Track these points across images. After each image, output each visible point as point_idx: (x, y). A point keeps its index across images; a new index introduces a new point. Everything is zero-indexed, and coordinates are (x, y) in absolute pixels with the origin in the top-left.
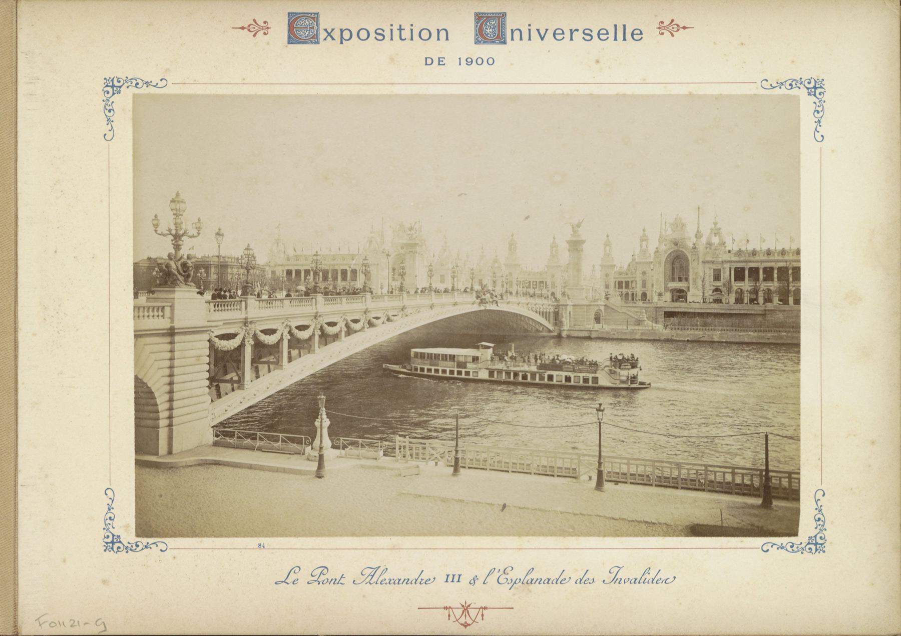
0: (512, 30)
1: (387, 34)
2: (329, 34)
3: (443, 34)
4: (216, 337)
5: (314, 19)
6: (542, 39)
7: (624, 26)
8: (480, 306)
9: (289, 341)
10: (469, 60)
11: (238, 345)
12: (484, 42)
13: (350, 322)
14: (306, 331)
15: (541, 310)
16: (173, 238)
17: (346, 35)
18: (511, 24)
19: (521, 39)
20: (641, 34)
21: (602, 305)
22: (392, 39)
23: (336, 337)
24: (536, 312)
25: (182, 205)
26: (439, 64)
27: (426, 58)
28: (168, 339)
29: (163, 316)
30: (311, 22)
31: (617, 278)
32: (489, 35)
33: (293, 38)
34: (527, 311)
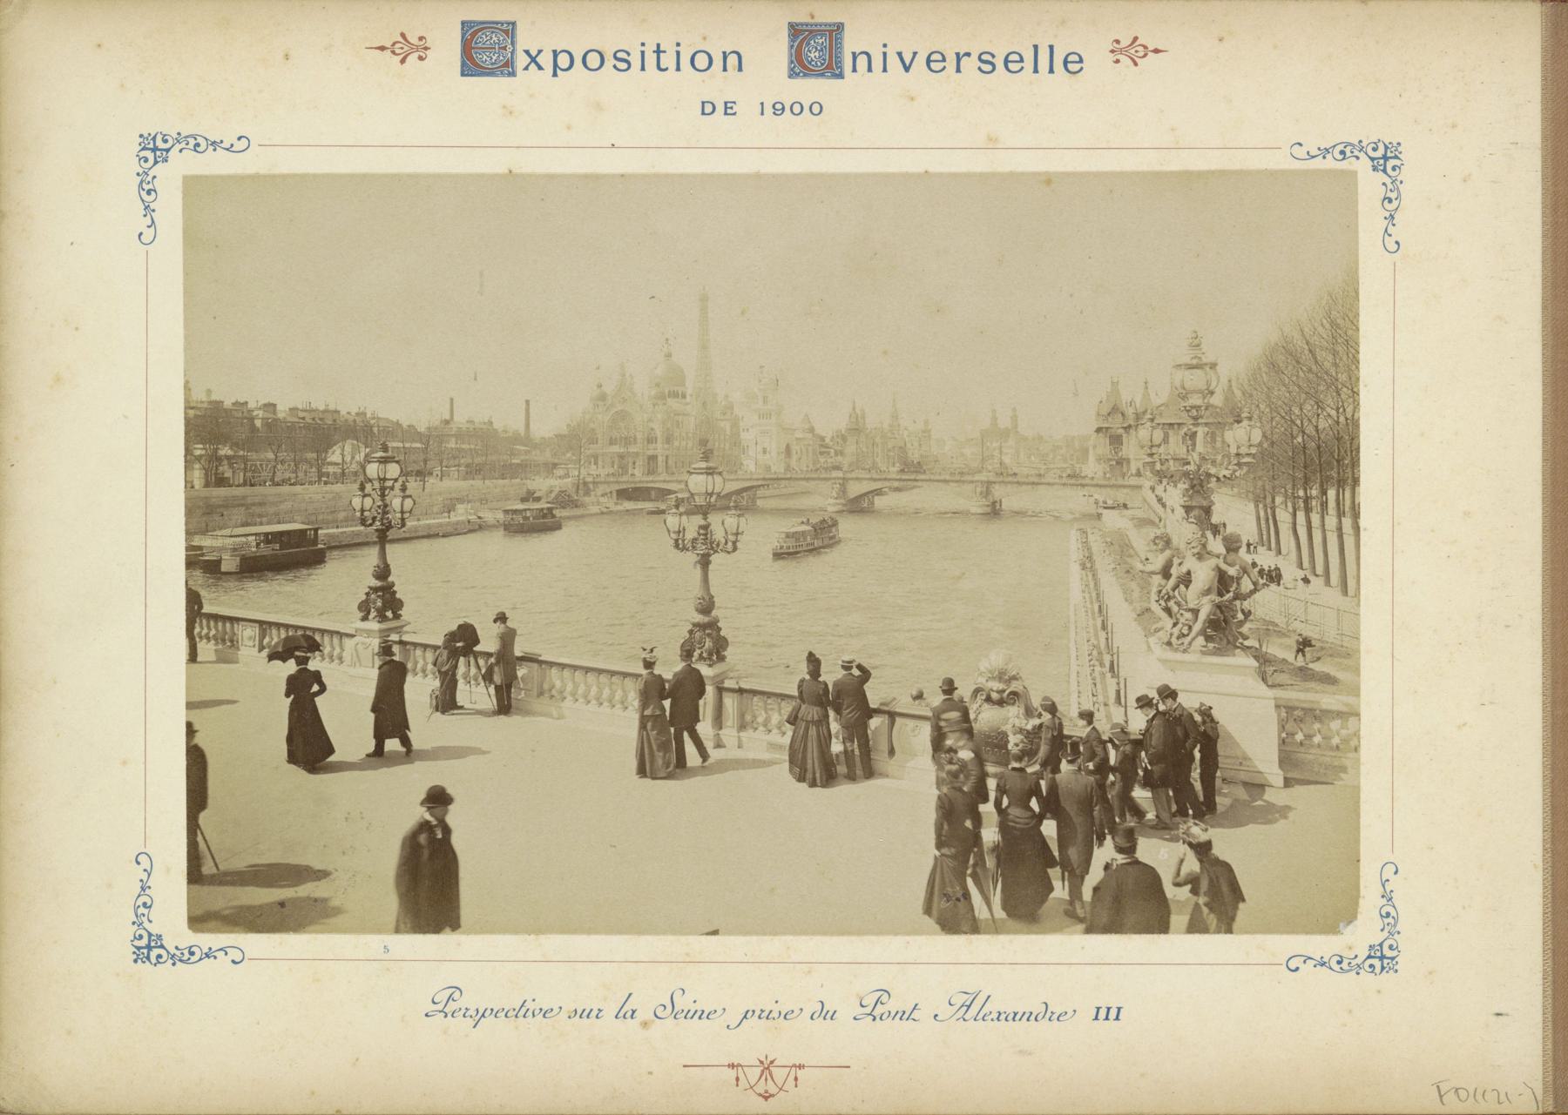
0: (854, 54)
1: (635, 60)
2: (533, 60)
3: (733, 59)
5: (506, 32)
6: (907, 69)
7: (1051, 47)
10: (779, 106)
12: (805, 75)
17: (563, 61)
18: (851, 43)
19: (870, 70)
20: (1081, 61)
22: (643, 69)
26: (726, 114)
27: (703, 103)
30: (502, 38)
32: (813, 63)
33: (471, 66)
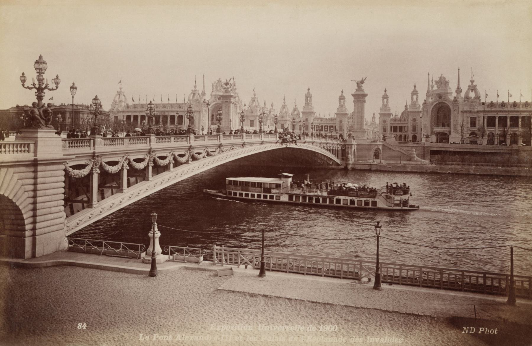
4: (70, 167)
8: (282, 144)
9: (128, 171)
11: (87, 173)
13: (177, 156)
14: (142, 163)
15: (331, 148)
16: (36, 91)
21: (380, 145)
23: (166, 168)
24: (327, 150)
25: (44, 65)
28: (32, 169)
29: (28, 151)
31: (392, 124)
34: (320, 149)
